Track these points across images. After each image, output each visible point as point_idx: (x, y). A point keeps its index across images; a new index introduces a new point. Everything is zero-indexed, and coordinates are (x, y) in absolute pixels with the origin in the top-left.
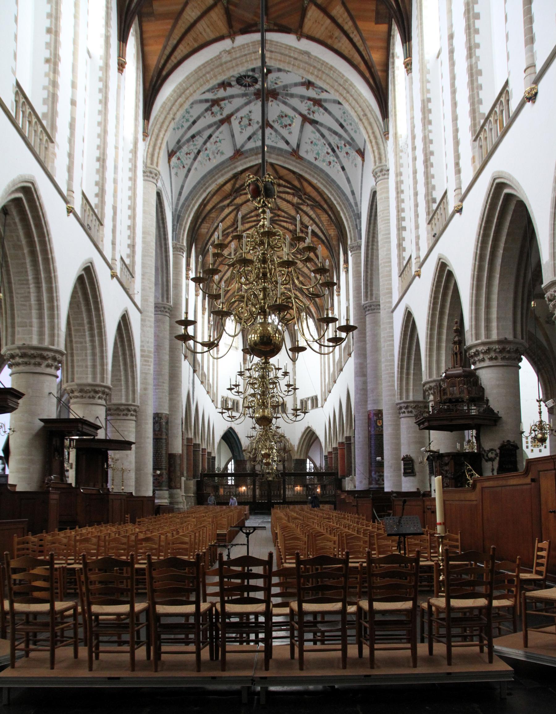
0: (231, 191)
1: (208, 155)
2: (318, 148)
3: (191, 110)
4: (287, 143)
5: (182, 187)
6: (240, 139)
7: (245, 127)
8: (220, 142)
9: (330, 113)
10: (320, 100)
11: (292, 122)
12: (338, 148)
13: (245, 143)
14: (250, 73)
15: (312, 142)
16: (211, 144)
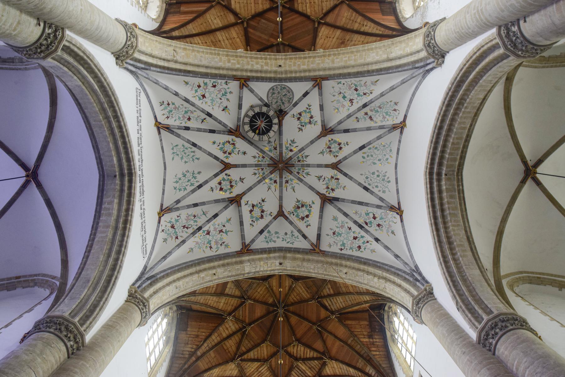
0: (236, 354)
1: (209, 242)
2: (342, 238)
3: (197, 175)
4: (305, 237)
5: (170, 253)
6: (250, 233)
7: (257, 219)
8: (226, 232)
9: (351, 178)
10: (340, 162)
11: (310, 211)
12: (366, 224)
13: (256, 237)
14: (264, 109)
15: (334, 233)
16: (215, 229)
